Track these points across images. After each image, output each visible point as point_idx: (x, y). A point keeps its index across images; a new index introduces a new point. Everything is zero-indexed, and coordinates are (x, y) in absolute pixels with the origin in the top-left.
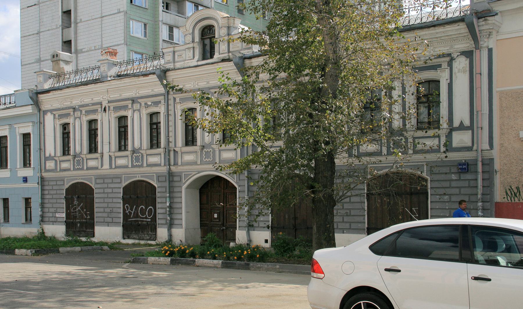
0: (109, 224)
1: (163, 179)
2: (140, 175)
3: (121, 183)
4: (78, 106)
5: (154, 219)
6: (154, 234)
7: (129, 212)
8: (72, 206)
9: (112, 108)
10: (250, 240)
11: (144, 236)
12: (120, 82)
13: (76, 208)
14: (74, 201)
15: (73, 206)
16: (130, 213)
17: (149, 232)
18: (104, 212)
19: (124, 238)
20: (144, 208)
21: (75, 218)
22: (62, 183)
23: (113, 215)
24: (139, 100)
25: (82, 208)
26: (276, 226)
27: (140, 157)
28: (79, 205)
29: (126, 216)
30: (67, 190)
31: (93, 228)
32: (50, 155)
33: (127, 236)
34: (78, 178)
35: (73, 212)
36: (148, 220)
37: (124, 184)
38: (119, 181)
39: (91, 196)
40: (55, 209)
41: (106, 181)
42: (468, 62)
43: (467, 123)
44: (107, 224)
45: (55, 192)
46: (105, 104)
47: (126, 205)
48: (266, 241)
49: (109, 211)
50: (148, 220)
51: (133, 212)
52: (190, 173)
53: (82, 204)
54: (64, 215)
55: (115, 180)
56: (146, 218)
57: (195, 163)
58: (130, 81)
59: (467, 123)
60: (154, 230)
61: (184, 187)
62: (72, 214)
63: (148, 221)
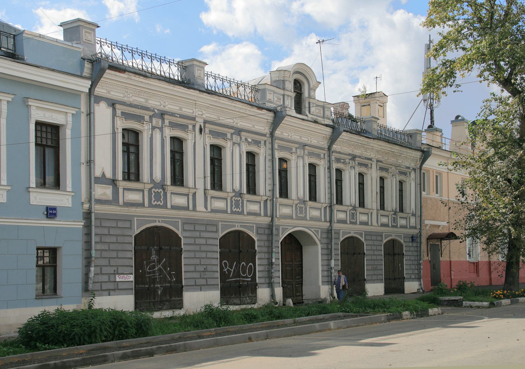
0: (202, 287)
1: (262, 231)
2: (239, 224)
3: (217, 232)
4: (158, 110)
5: (254, 278)
6: (254, 296)
7: (228, 270)
8: (146, 263)
9: (207, 130)
11: (245, 299)
12: (230, 104)
13: (154, 267)
14: (151, 255)
15: (150, 263)
16: (229, 272)
17: (249, 294)
18: (195, 271)
20: (245, 265)
21: (154, 281)
22: (127, 225)
23: (208, 275)
27: (240, 202)
28: (159, 262)
29: (223, 276)
30: (136, 237)
34: (157, 220)
35: (149, 273)
36: (248, 279)
37: (221, 235)
38: (214, 229)
40: (115, 268)
41: (198, 228)
44: (199, 287)
45: (114, 239)
47: (224, 262)
49: (203, 270)
50: (248, 279)
51: (232, 270)
52: (286, 227)
53: (164, 259)
54: (132, 278)
55: (210, 228)
56: (247, 277)
57: (291, 217)
58: (241, 107)
60: (254, 291)
61: (280, 241)
62: (147, 275)
63: (248, 281)
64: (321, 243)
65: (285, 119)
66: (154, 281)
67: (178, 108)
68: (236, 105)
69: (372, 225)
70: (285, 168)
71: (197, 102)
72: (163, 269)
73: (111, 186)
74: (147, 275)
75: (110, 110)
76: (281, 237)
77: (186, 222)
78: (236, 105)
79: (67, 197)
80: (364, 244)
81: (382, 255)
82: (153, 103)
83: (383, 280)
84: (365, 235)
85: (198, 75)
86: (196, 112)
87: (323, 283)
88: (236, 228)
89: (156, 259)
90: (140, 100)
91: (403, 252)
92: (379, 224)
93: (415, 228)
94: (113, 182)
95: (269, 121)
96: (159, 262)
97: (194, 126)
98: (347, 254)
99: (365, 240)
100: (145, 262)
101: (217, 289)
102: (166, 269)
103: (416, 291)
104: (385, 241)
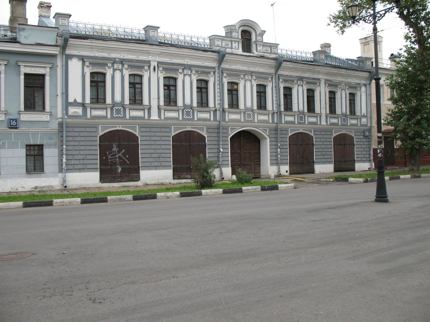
1: (212, 131)
2: (190, 127)
4: (119, 59)
9: (161, 69)
10: (279, 171)
13: (115, 155)
15: (112, 153)
19: (174, 178)
21: (115, 164)
24: (192, 68)
25: (124, 154)
26: (292, 162)
28: (119, 151)
30: (100, 137)
31: (139, 173)
32: (75, 100)
33: (178, 177)
37: (173, 134)
39: (135, 143)
42: (365, 89)
43: (365, 115)
46: (154, 64)
48: (287, 171)
53: (124, 150)
59: (365, 115)
62: (109, 160)
64: (270, 138)
65: (226, 56)
66: (115, 164)
67: (135, 56)
68: (183, 51)
69: (320, 125)
70: (236, 88)
71: (149, 52)
72: (122, 156)
73: (81, 107)
74: (109, 160)
75: (80, 63)
76: (231, 134)
77: (142, 127)
78: (183, 51)
79: (47, 115)
80: (313, 137)
81: (332, 145)
82: (113, 55)
83: (333, 162)
84: (314, 131)
85: (153, 34)
86: (150, 58)
87: (271, 164)
88: (188, 129)
89: (116, 150)
90: (106, 55)
91: (354, 142)
92: (329, 124)
93: (366, 125)
94: (83, 105)
95: (215, 59)
96: (119, 151)
97: (149, 67)
98: (296, 145)
99: (315, 134)
100: (107, 152)
101: (170, 169)
102: (125, 157)
103: (367, 169)
104: (334, 135)
